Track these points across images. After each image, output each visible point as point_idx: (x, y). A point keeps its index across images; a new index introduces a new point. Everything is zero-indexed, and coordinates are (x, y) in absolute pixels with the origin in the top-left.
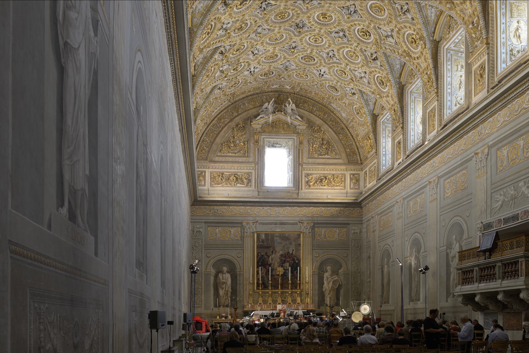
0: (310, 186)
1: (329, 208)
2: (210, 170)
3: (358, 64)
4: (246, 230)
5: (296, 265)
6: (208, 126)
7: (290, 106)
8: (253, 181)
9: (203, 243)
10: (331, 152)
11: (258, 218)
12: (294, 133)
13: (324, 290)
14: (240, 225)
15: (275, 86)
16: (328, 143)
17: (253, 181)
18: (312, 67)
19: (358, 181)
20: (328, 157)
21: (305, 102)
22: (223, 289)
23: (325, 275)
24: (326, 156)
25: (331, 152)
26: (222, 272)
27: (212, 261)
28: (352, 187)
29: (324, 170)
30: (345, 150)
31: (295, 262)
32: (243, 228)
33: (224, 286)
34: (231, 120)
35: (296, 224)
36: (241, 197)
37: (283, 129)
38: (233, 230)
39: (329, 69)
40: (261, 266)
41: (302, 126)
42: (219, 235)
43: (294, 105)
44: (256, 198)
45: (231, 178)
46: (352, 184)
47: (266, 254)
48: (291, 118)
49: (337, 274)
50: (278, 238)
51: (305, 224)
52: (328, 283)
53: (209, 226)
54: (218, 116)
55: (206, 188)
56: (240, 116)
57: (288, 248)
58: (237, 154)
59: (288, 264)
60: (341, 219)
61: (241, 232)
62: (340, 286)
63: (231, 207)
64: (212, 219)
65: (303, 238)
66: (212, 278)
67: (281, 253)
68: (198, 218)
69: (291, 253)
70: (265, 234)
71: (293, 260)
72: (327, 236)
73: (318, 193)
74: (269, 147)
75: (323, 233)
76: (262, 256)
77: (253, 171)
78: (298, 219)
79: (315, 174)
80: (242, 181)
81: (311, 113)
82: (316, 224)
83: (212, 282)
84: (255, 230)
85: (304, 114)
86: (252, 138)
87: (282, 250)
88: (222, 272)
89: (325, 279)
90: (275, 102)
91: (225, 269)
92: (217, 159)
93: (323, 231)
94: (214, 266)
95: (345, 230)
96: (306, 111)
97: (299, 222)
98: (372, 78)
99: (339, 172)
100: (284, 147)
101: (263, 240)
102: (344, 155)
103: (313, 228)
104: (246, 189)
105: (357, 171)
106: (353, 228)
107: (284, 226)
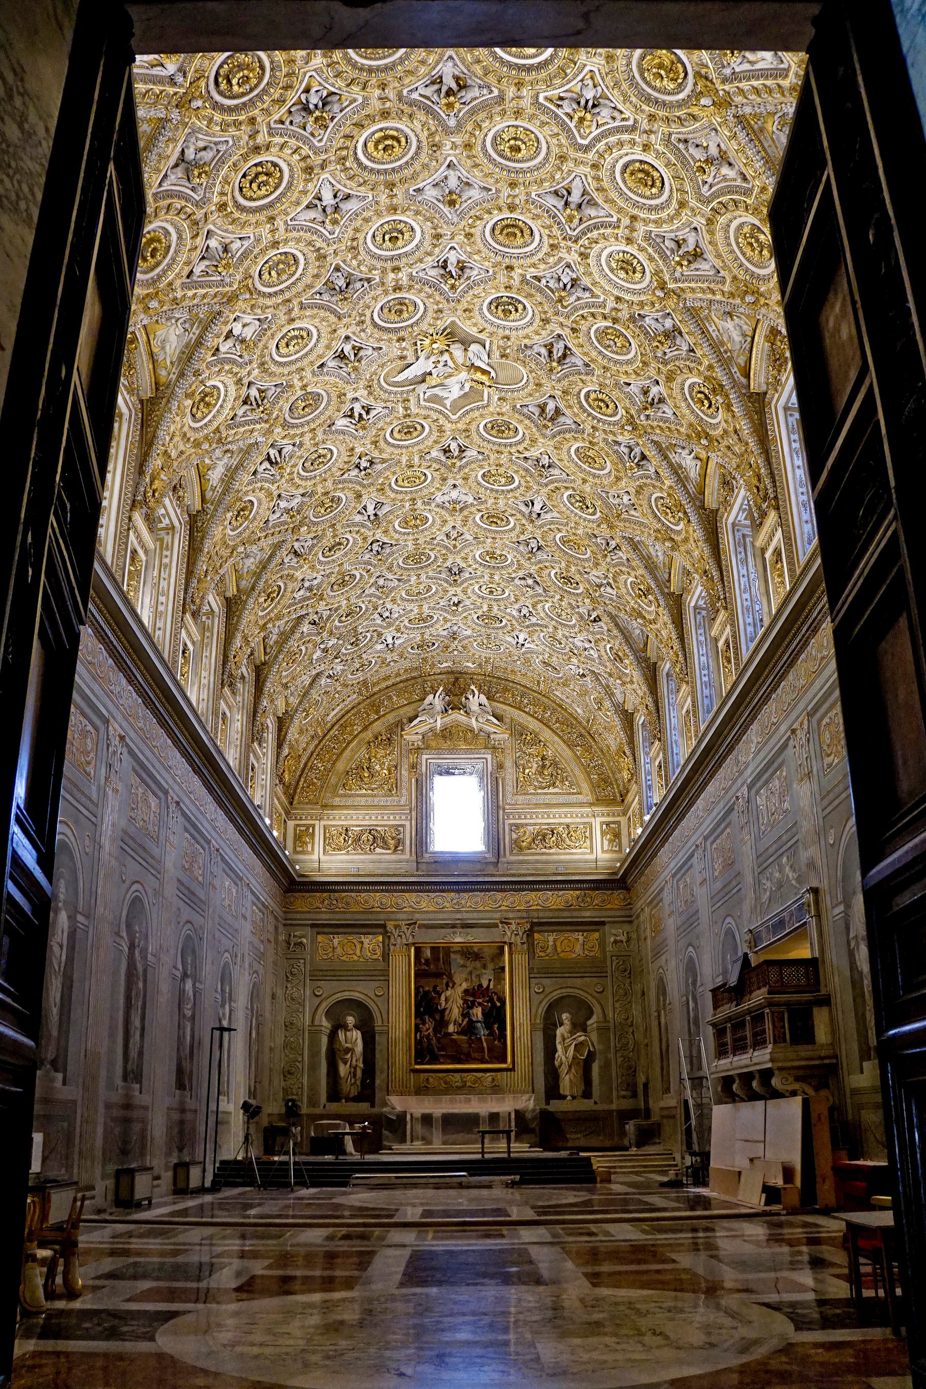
0: (521, 848)
1: (561, 893)
2: (323, 823)
3: (574, 626)
4: (392, 940)
6: (320, 742)
7: (476, 700)
8: (408, 842)
9: (308, 966)
10: (562, 782)
11: (417, 916)
12: (486, 748)
13: (557, 1063)
14: (380, 930)
15: (445, 665)
16: (555, 764)
17: (408, 842)
18: (500, 632)
19: (617, 835)
20: (556, 790)
21: (506, 690)
22: (345, 1063)
23: (558, 1032)
24: (552, 790)
25: (562, 782)
26: (345, 1027)
27: (324, 1006)
28: (606, 848)
29: (549, 817)
30: (589, 776)
31: (494, 1004)
32: (386, 934)
33: (349, 1056)
34: (365, 728)
35: (496, 926)
36: (382, 875)
37: (465, 740)
38: (366, 940)
39: (530, 634)
40: (425, 1013)
41: (501, 735)
42: (339, 951)
43: (482, 696)
44: (412, 876)
45: (364, 837)
46: (606, 843)
47: (435, 987)
48: (477, 720)
49: (585, 1030)
50: (458, 957)
51: (513, 927)
52: (566, 1049)
53: (318, 933)
54: (341, 722)
55: (315, 857)
56: (382, 719)
57: (479, 976)
58: (376, 792)
59: (480, 1009)
60: (588, 914)
61: (383, 942)
62: (591, 1056)
63: (363, 895)
64: (324, 918)
65: (511, 954)
66: (325, 1040)
67: (465, 986)
68: (298, 916)
69: (485, 986)
70: (432, 948)
71: (491, 1000)
72: (559, 950)
73: (537, 862)
74: (441, 774)
75: (551, 943)
76: (427, 993)
77: (407, 824)
78: (498, 915)
79: (531, 825)
80: (385, 843)
81: (520, 709)
82: (536, 926)
83: (324, 1049)
84: (411, 941)
85: (505, 711)
86: (404, 759)
87: (466, 980)
88: (345, 1027)
89: (558, 1039)
90: (448, 692)
91: (351, 1020)
92: (337, 801)
93: (551, 939)
94: (329, 1014)
95: (596, 935)
96: (509, 705)
97: (502, 923)
98: (602, 650)
99: (578, 820)
100: (471, 774)
101: (427, 960)
102: (585, 786)
103: (530, 933)
104: (394, 857)
105: (614, 815)
106: (614, 931)
107: (469, 930)
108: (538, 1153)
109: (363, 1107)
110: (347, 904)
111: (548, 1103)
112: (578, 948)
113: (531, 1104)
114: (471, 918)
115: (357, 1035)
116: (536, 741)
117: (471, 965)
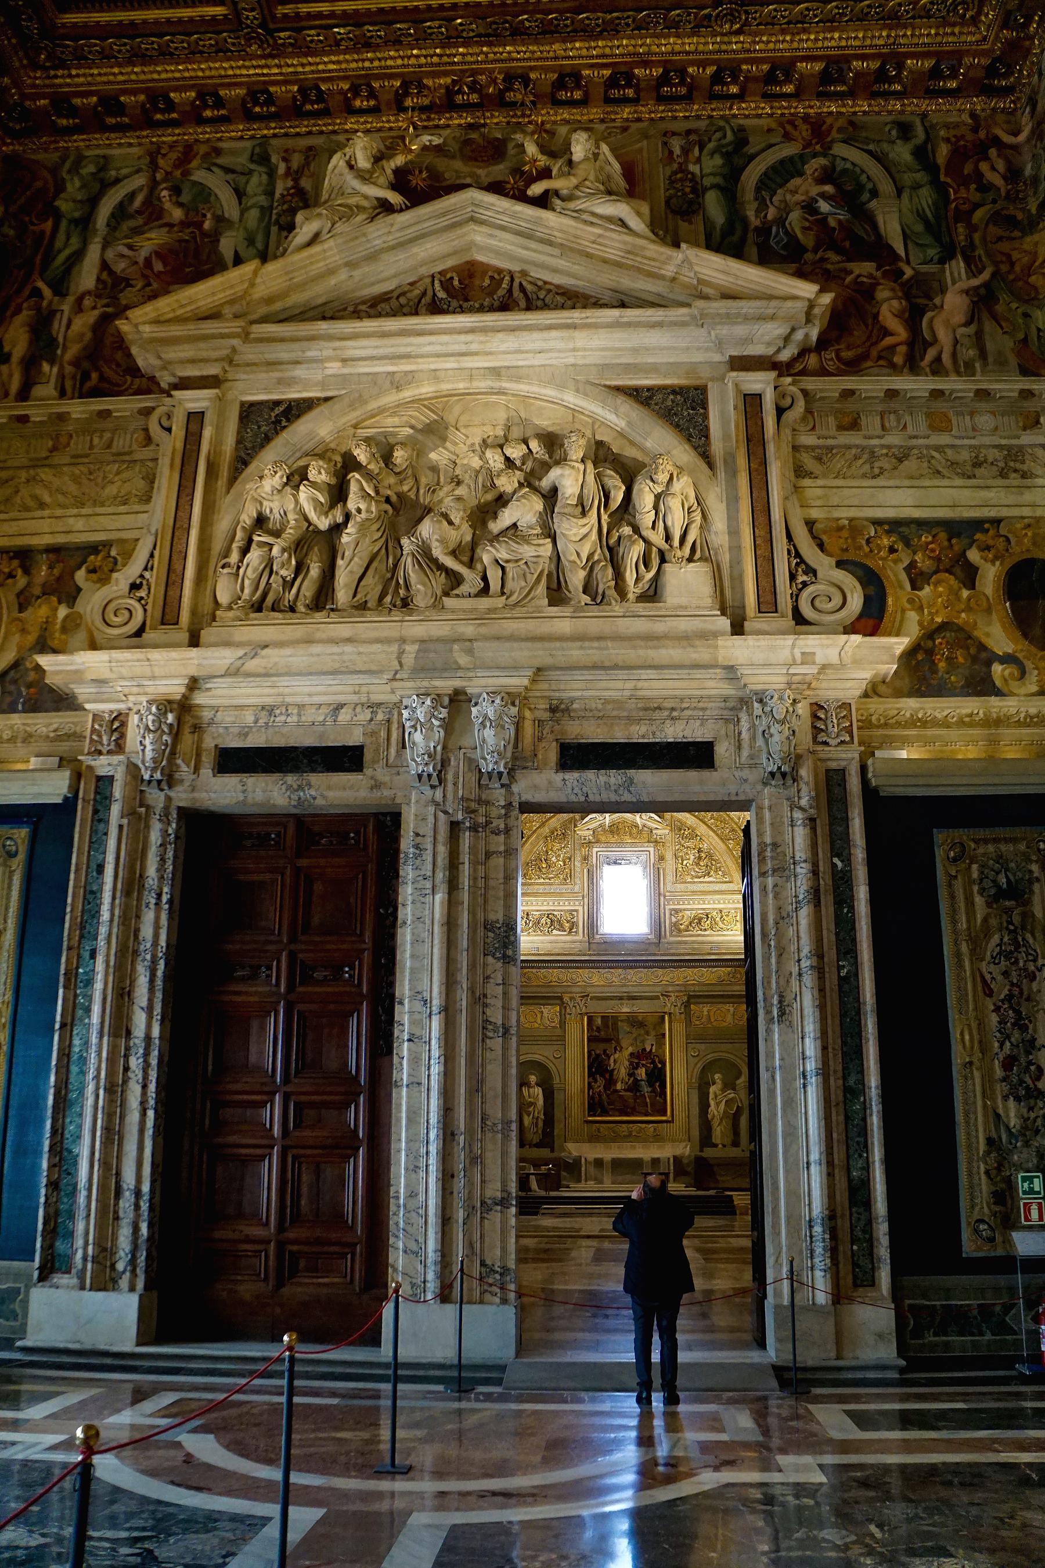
0: (680, 930)
5: (657, 1076)
35: (657, 998)
51: (673, 999)
57: (643, 1042)
65: (670, 1022)
73: (694, 942)
82: (692, 998)
103: (687, 1005)
108: (692, 1191)
109: (544, 1153)
110: (529, 978)
111: (701, 1151)
112: (729, 1018)
113: (687, 1151)
114: (635, 991)
115: (538, 1091)
116: (693, 835)
117: (635, 1032)
